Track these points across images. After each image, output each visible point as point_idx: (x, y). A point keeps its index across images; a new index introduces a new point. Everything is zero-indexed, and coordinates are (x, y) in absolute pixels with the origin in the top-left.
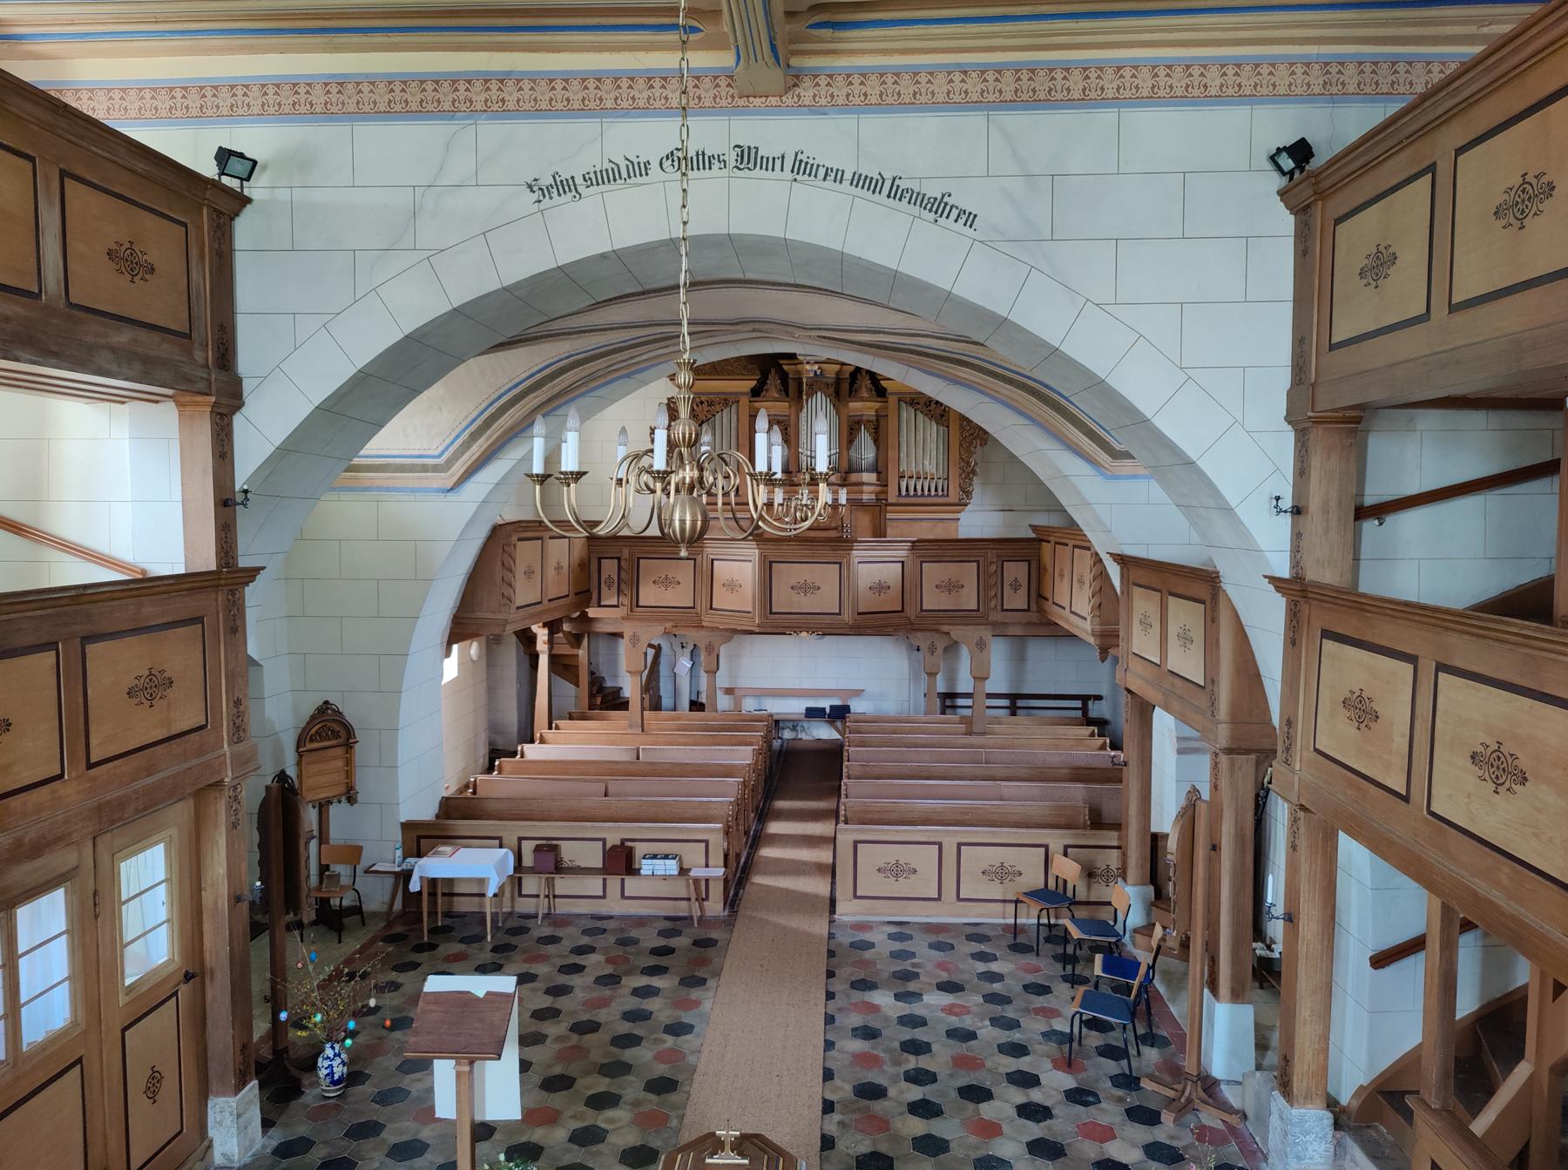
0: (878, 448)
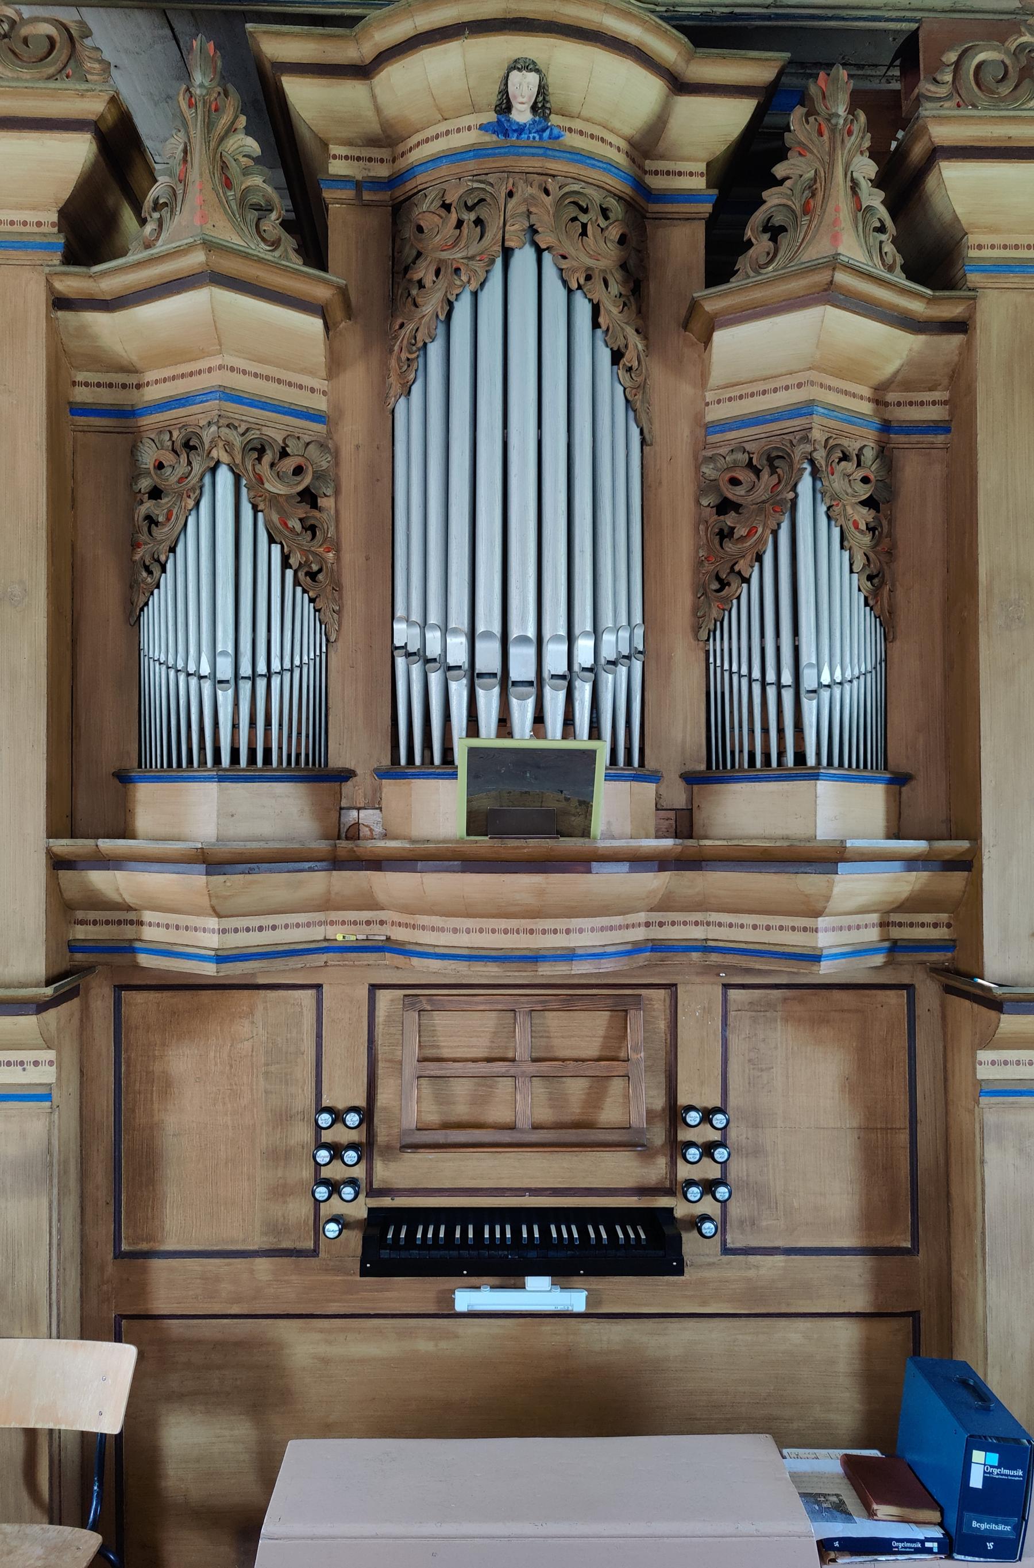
0: (887, 623)
